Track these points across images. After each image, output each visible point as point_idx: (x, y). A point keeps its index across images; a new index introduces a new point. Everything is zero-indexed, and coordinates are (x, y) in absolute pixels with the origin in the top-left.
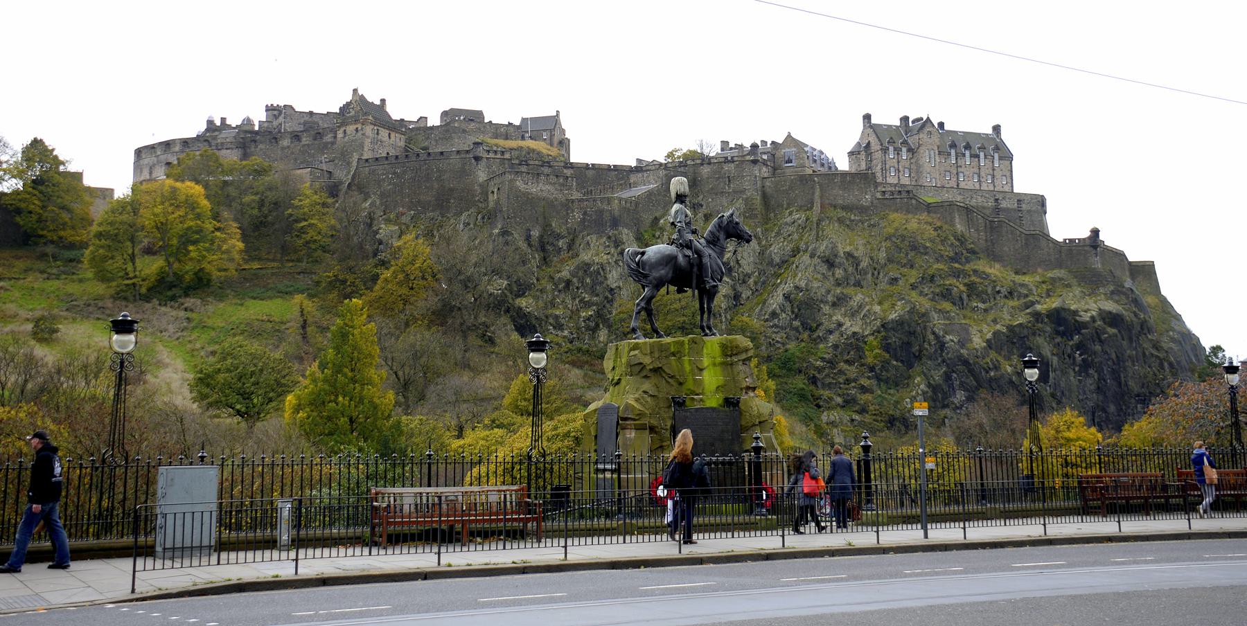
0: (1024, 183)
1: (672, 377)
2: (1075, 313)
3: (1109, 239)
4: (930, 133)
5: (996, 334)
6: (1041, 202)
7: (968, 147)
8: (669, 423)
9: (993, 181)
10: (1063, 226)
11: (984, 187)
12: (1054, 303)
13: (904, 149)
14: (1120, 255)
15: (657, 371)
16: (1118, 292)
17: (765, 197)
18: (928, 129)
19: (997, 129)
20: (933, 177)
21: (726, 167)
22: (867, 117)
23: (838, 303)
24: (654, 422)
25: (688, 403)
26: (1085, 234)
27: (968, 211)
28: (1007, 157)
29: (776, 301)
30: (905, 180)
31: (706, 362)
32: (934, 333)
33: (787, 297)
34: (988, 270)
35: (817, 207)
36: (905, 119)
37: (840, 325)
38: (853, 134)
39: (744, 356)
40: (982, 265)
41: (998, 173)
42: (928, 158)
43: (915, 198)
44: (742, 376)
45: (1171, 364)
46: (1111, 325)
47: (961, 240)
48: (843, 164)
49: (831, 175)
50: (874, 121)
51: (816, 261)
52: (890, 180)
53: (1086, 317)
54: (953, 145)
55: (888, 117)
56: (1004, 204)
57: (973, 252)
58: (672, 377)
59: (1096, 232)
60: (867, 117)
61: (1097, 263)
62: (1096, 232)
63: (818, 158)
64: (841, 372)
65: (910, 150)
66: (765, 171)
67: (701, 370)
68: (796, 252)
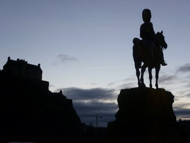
0: (44, 79)
22: (9, 58)
28: (41, 72)
36: (18, 59)
55: (14, 58)
60: (9, 58)
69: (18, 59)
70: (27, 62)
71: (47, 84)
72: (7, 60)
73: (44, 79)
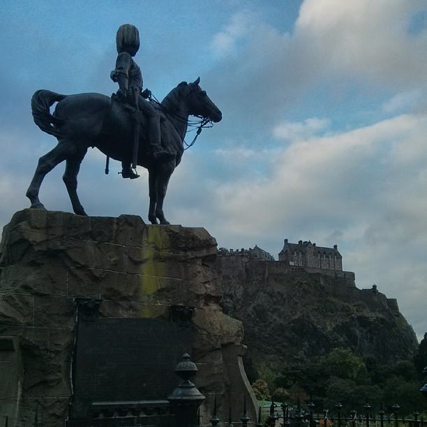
1: (83, 267)
2: (368, 318)
3: (380, 290)
4: (310, 247)
5: (337, 326)
6: (353, 275)
7: (325, 253)
8: (64, 341)
10: (361, 284)
12: (360, 314)
15: (54, 255)
16: (383, 310)
17: (246, 270)
18: (309, 245)
19: (335, 247)
20: (312, 264)
21: (232, 257)
22: (286, 241)
23: (275, 311)
24: (32, 338)
25: (106, 309)
27: (326, 277)
28: (341, 257)
29: (250, 309)
30: (301, 265)
31: (147, 253)
32: (313, 325)
33: (254, 308)
34: (334, 300)
35: (267, 275)
36: (300, 242)
37: (275, 320)
38: (280, 248)
39: (204, 253)
40: (333, 299)
41: (336, 264)
42: (310, 257)
43: (305, 271)
44: (200, 279)
45: (403, 339)
46: (382, 323)
47: (322, 288)
48: (277, 259)
49: (272, 261)
50: (289, 242)
51: (266, 295)
53: (372, 320)
54: (319, 252)
55: (294, 241)
56: (338, 276)
57: (327, 293)
58: (83, 267)
60: (286, 241)
61: (376, 299)
63: (267, 255)
64: (276, 339)
65: (302, 253)
66: (246, 260)
67: (137, 263)
68: (258, 291)
69: (300, 242)
70: (314, 244)
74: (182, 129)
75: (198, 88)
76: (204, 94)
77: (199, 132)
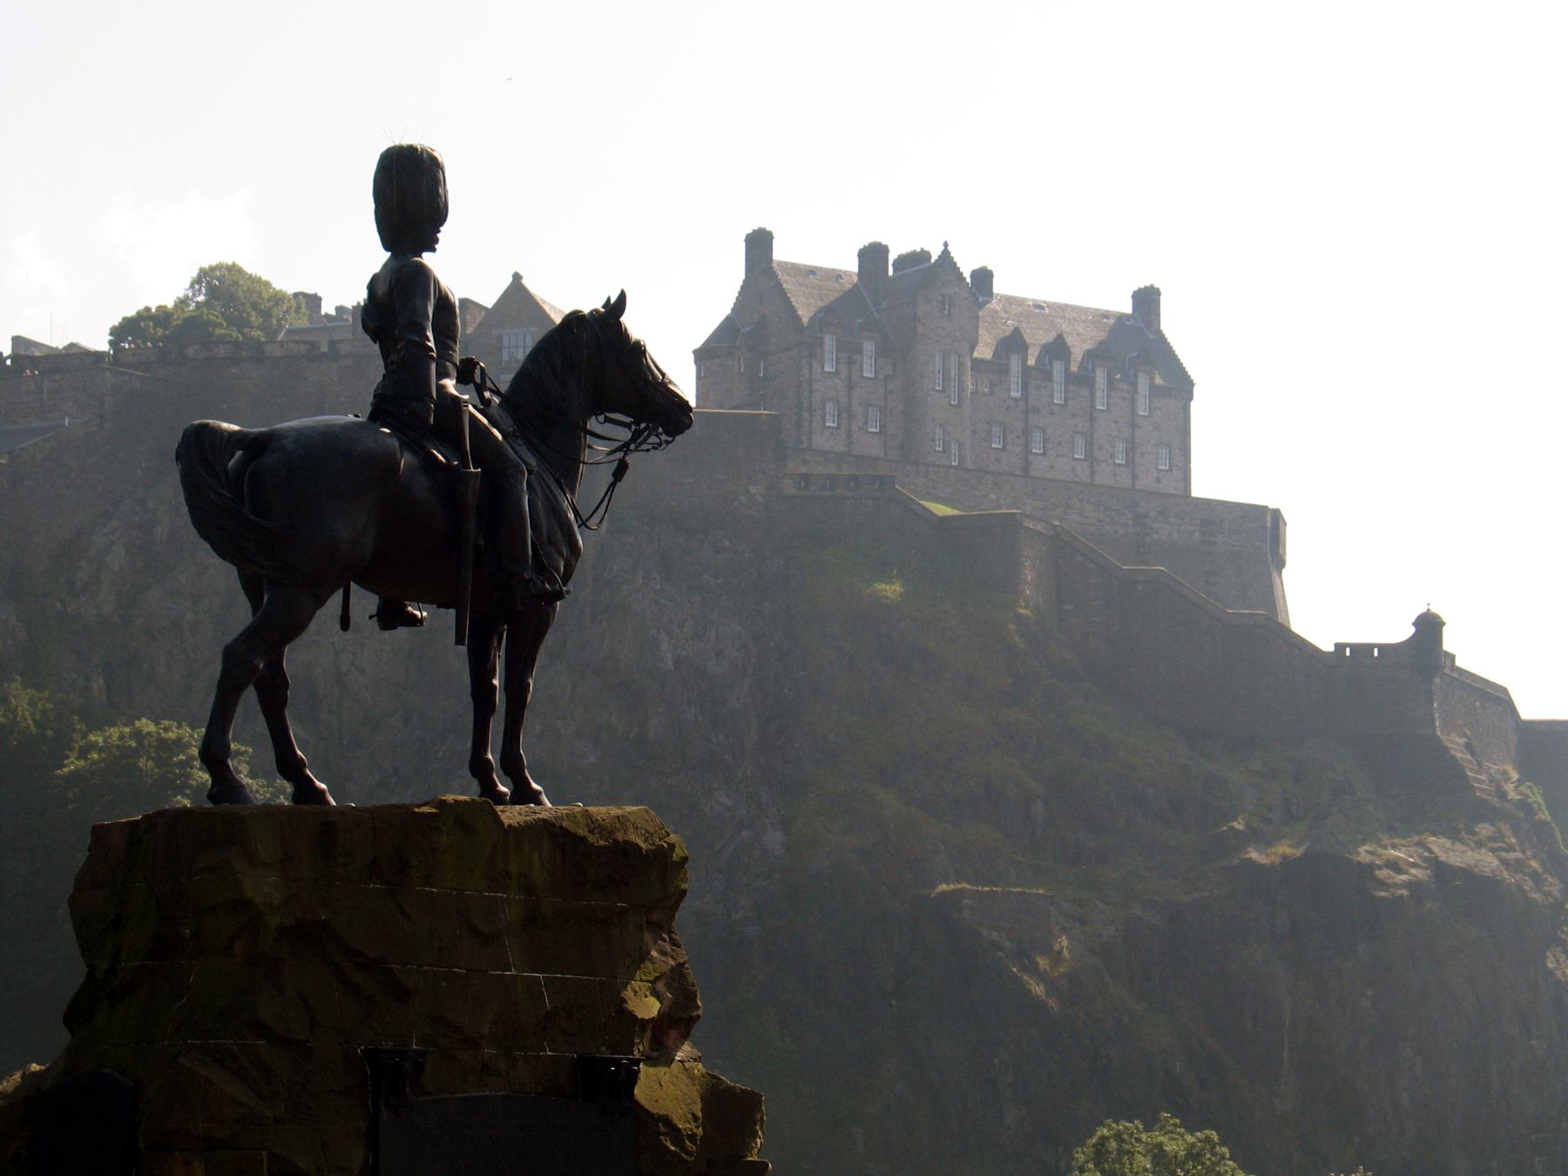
0: (1217, 473)
3: (1467, 648)
9: (1130, 462)
11: (1104, 477)
13: (869, 347)
14: (1495, 698)
19: (1147, 300)
22: (759, 243)
26: (1400, 631)
28: (1180, 387)
36: (873, 255)
50: (782, 252)
52: (822, 441)
55: (821, 244)
59: (1429, 626)
60: (759, 243)
62: (1429, 626)
69: (873, 255)
70: (983, 277)
71: (1256, 536)
72: (731, 276)
73: (1217, 473)
74: (566, 469)
75: (622, 334)
76: (638, 350)
77: (620, 471)
